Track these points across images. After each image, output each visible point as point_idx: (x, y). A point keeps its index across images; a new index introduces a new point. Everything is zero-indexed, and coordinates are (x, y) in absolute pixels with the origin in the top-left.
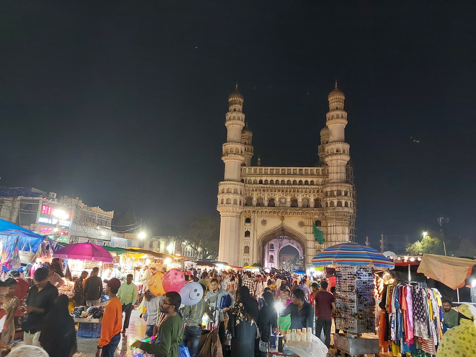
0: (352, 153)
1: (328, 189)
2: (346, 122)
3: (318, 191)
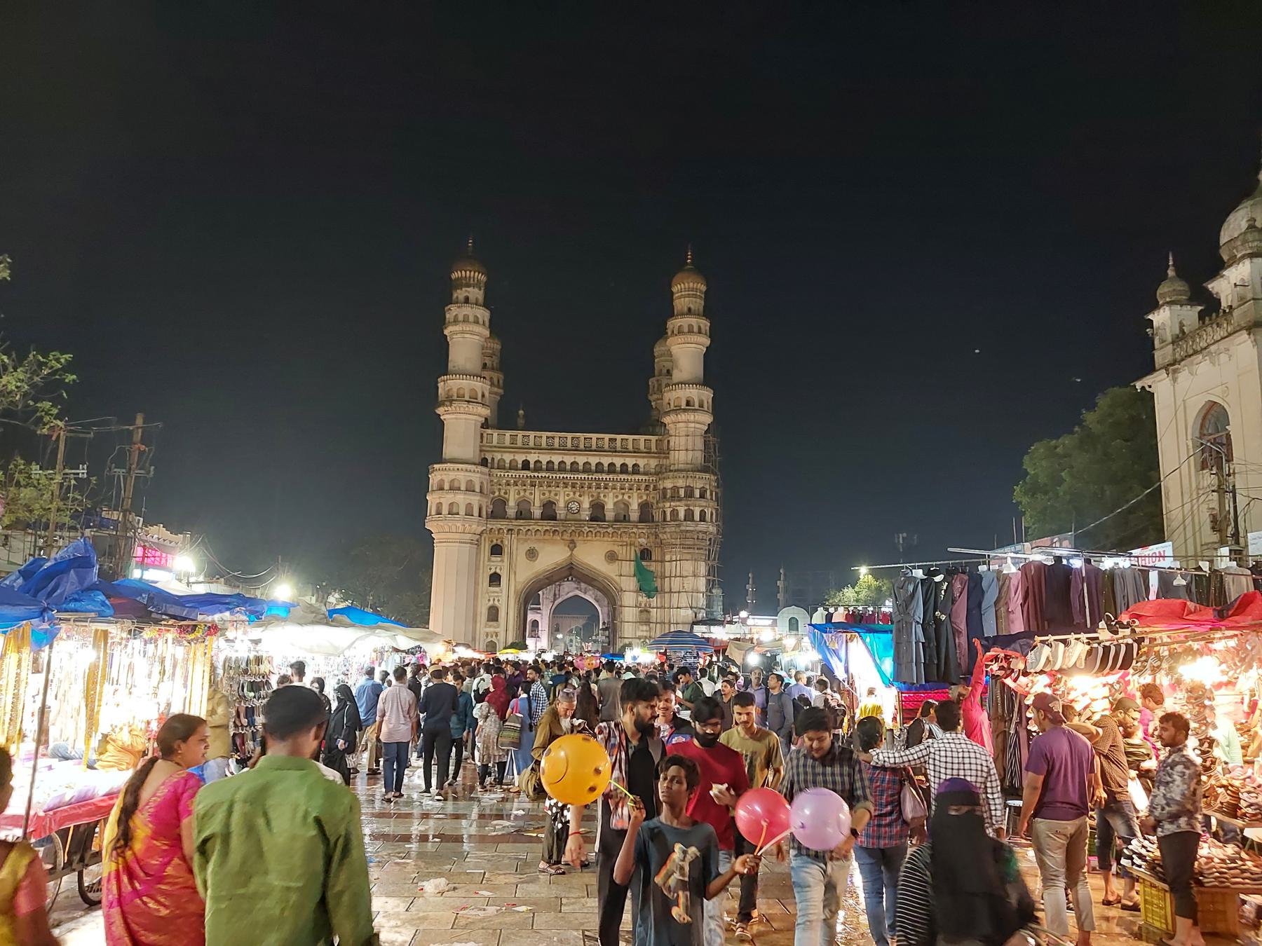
0: (718, 408)
1: (668, 484)
2: (707, 342)
3: (647, 488)
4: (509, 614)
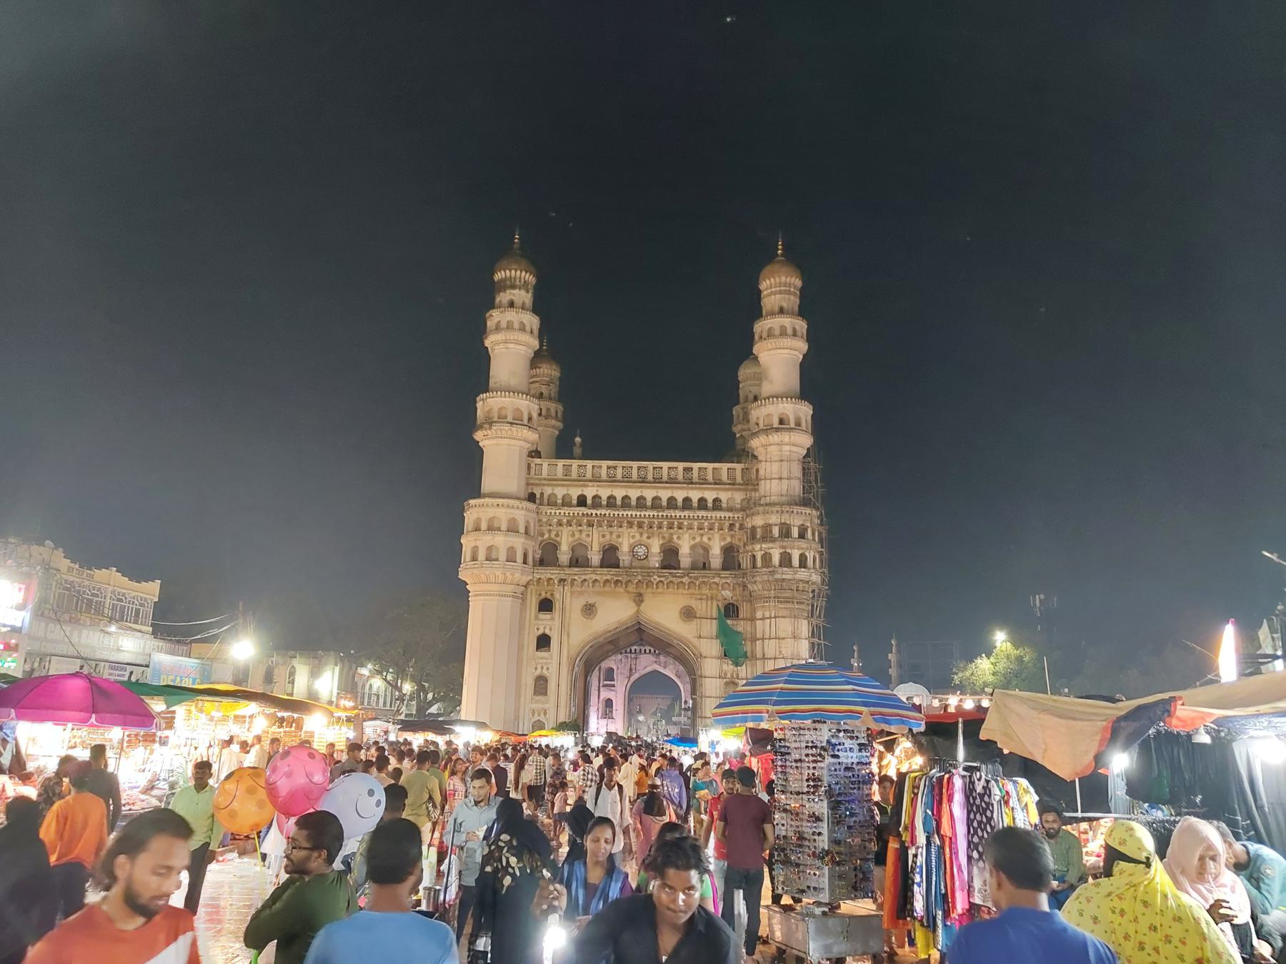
0: (819, 427)
1: (758, 521)
2: (803, 346)
3: (731, 526)
4: (561, 685)
